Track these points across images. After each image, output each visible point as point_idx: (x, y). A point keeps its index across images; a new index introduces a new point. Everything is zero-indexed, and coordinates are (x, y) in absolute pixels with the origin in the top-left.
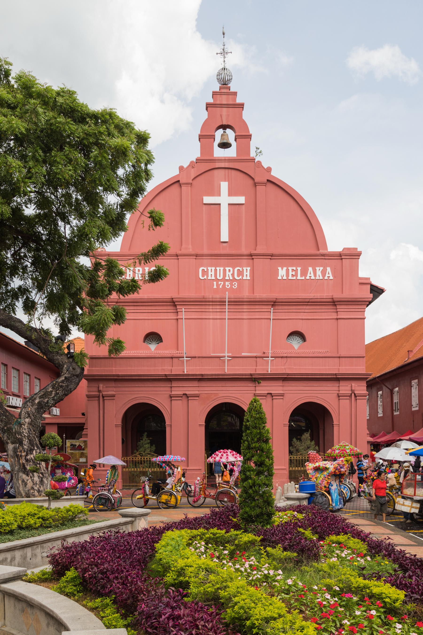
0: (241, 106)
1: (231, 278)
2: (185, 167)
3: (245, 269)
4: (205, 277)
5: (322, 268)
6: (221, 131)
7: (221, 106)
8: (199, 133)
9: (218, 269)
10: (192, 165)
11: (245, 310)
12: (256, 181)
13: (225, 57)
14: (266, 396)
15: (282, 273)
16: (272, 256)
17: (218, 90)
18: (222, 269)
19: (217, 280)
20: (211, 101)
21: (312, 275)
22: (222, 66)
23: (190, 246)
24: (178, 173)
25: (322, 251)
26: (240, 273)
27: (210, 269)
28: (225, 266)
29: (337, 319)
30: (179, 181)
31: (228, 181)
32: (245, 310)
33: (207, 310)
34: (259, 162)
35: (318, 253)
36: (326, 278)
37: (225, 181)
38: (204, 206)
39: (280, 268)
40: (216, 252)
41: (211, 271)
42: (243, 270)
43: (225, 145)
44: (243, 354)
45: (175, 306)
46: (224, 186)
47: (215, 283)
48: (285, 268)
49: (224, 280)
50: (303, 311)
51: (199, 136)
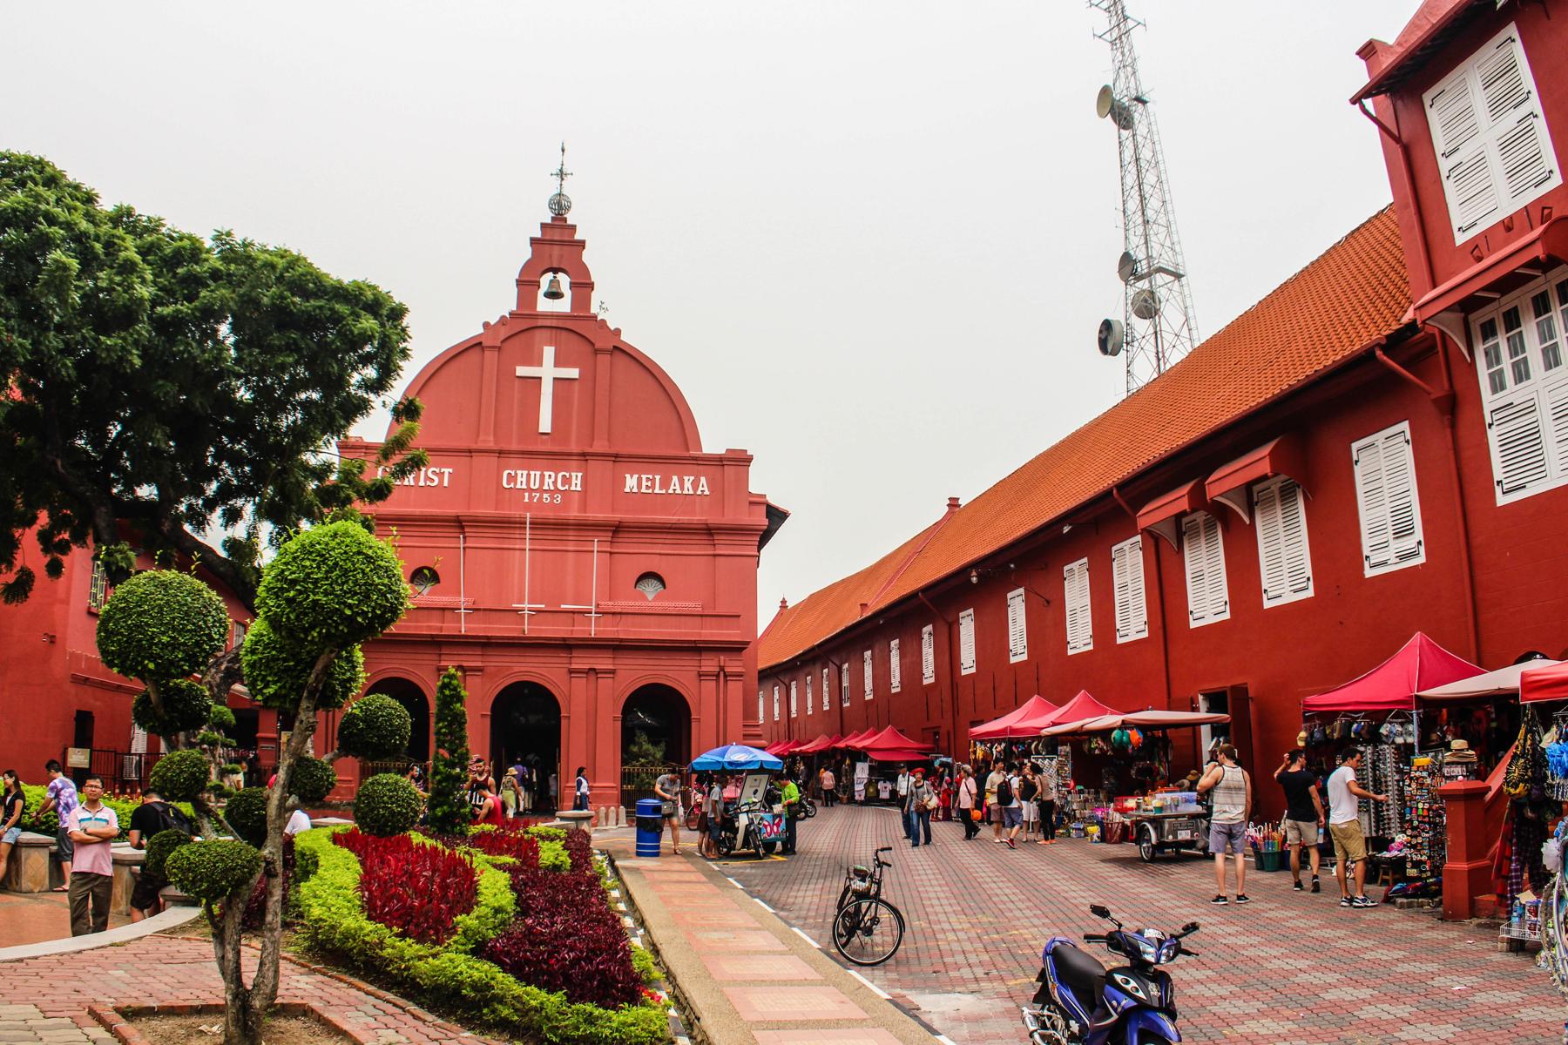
0: (582, 244)
1: (552, 488)
2: (492, 323)
3: (574, 474)
4: (512, 485)
5: (692, 478)
6: (550, 276)
7: (552, 242)
8: (517, 277)
9: (532, 473)
10: (503, 320)
11: (571, 538)
12: (598, 346)
13: (562, 179)
14: (587, 673)
15: (631, 482)
16: (616, 458)
17: (549, 221)
18: (538, 473)
19: (530, 490)
20: (538, 234)
21: (678, 487)
22: (558, 191)
23: (492, 438)
24: (481, 330)
25: (693, 453)
26: (566, 481)
27: (519, 472)
28: (543, 470)
29: (715, 555)
30: (481, 343)
31: (556, 345)
32: (571, 538)
33: (512, 536)
34: (603, 321)
35: (686, 454)
36: (699, 492)
37: (551, 345)
38: (517, 383)
39: (628, 476)
40: (530, 448)
41: (521, 475)
42: (571, 476)
43: (554, 295)
44: (562, 606)
45: (462, 527)
46: (549, 352)
47: (527, 494)
48: (636, 476)
49: (541, 490)
50: (662, 541)
51: (517, 281)
